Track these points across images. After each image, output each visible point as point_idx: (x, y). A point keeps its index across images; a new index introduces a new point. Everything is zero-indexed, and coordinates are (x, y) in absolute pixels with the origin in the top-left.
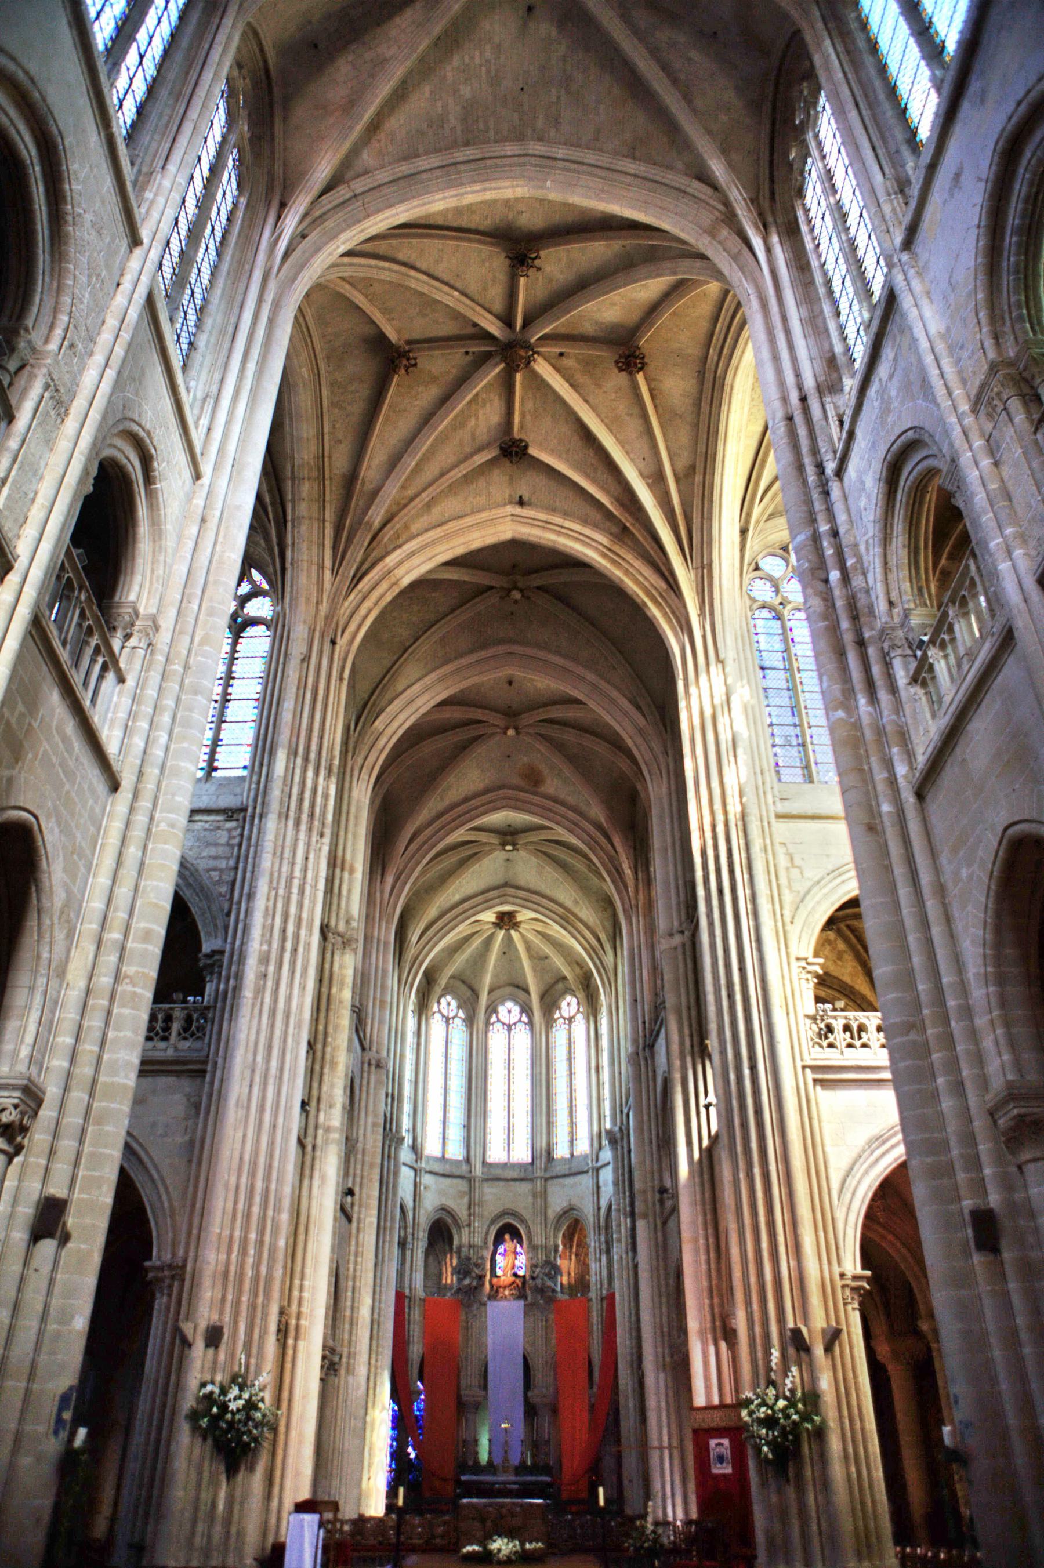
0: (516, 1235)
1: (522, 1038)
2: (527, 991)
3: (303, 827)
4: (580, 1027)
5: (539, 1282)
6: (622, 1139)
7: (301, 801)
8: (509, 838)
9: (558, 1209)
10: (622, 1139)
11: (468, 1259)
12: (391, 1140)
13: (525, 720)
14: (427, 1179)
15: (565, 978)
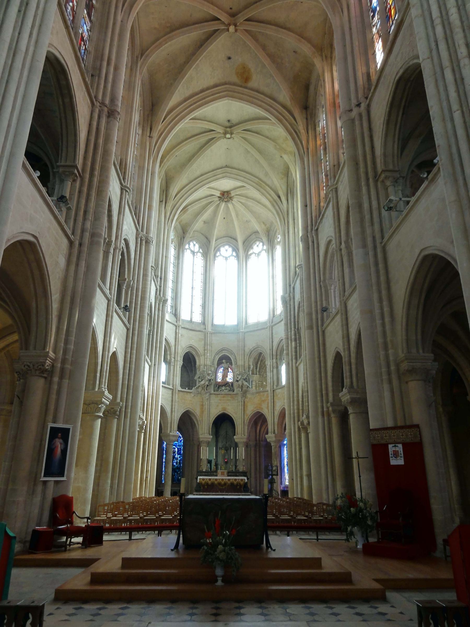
2: (236, 240)
5: (240, 383)
8: (228, 129)
9: (251, 348)
10: (290, 300)
11: (204, 371)
13: (241, 19)
14: (181, 331)
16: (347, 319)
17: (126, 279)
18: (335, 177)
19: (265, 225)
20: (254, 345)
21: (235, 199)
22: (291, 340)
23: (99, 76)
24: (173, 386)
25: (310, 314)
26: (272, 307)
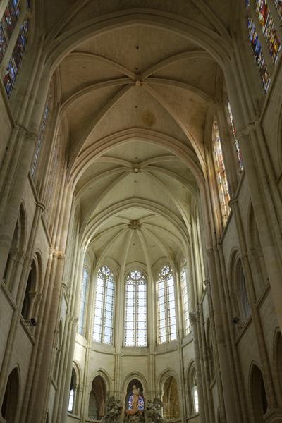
1: (142, 288)
5: (151, 411)
6: (199, 317)
8: (136, 165)
10: (199, 317)
11: (113, 398)
12: (71, 320)
15: (165, 257)
16: (261, 327)
17: (35, 293)
18: (234, 192)
19: (172, 250)
20: (164, 368)
21: (143, 227)
22: (203, 359)
23: (22, 106)
24: (81, 417)
25: (221, 327)
26: (180, 327)
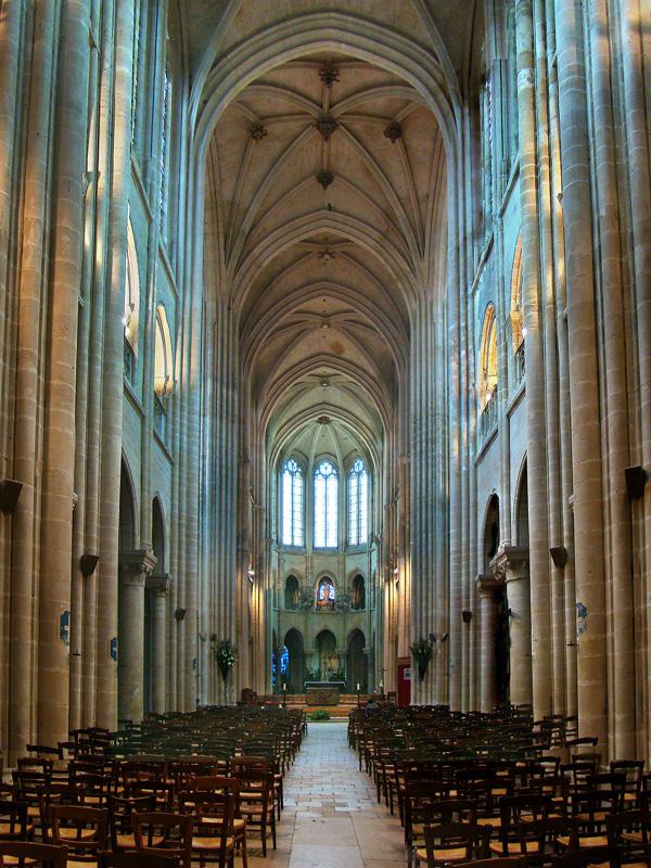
0: (330, 582)
1: (333, 483)
2: (335, 456)
3: (224, 421)
4: (364, 479)
7: (221, 406)
